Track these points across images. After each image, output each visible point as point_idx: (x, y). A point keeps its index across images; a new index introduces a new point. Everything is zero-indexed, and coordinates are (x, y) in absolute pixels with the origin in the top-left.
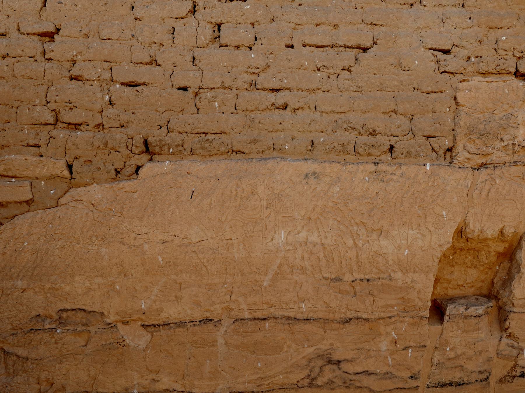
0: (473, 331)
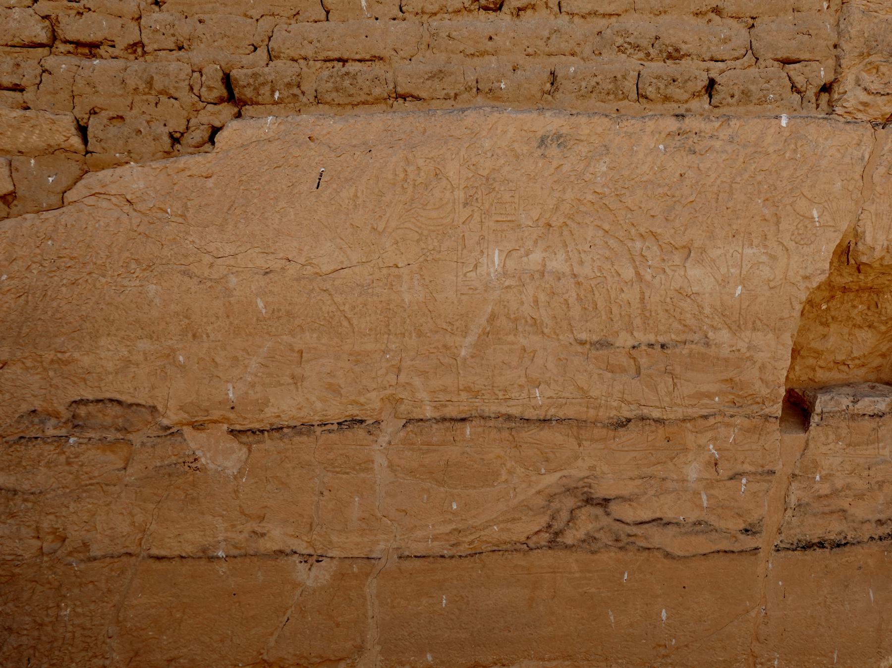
0: (867, 444)
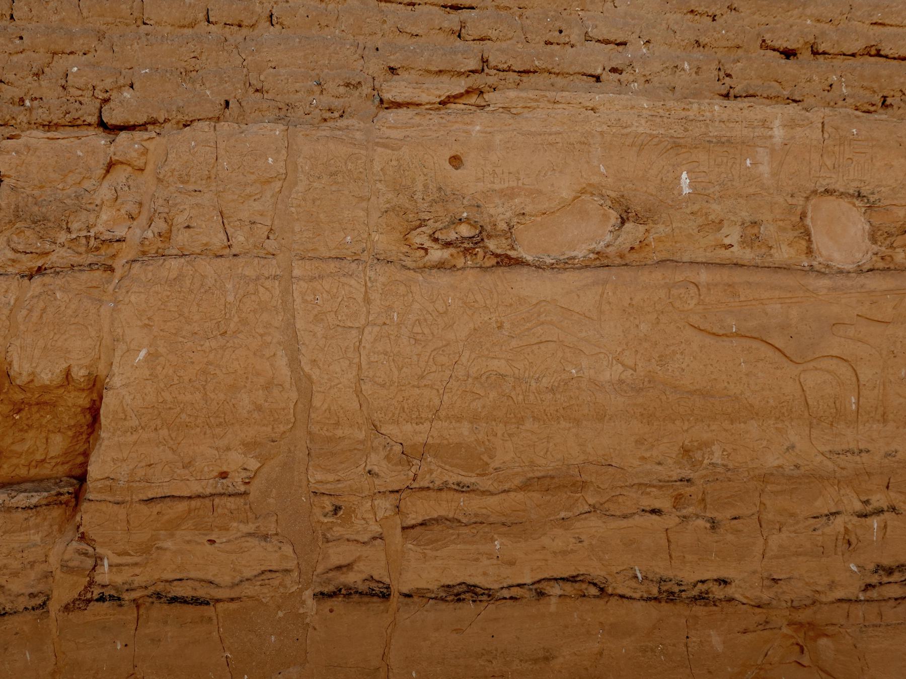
0: (21, 531)
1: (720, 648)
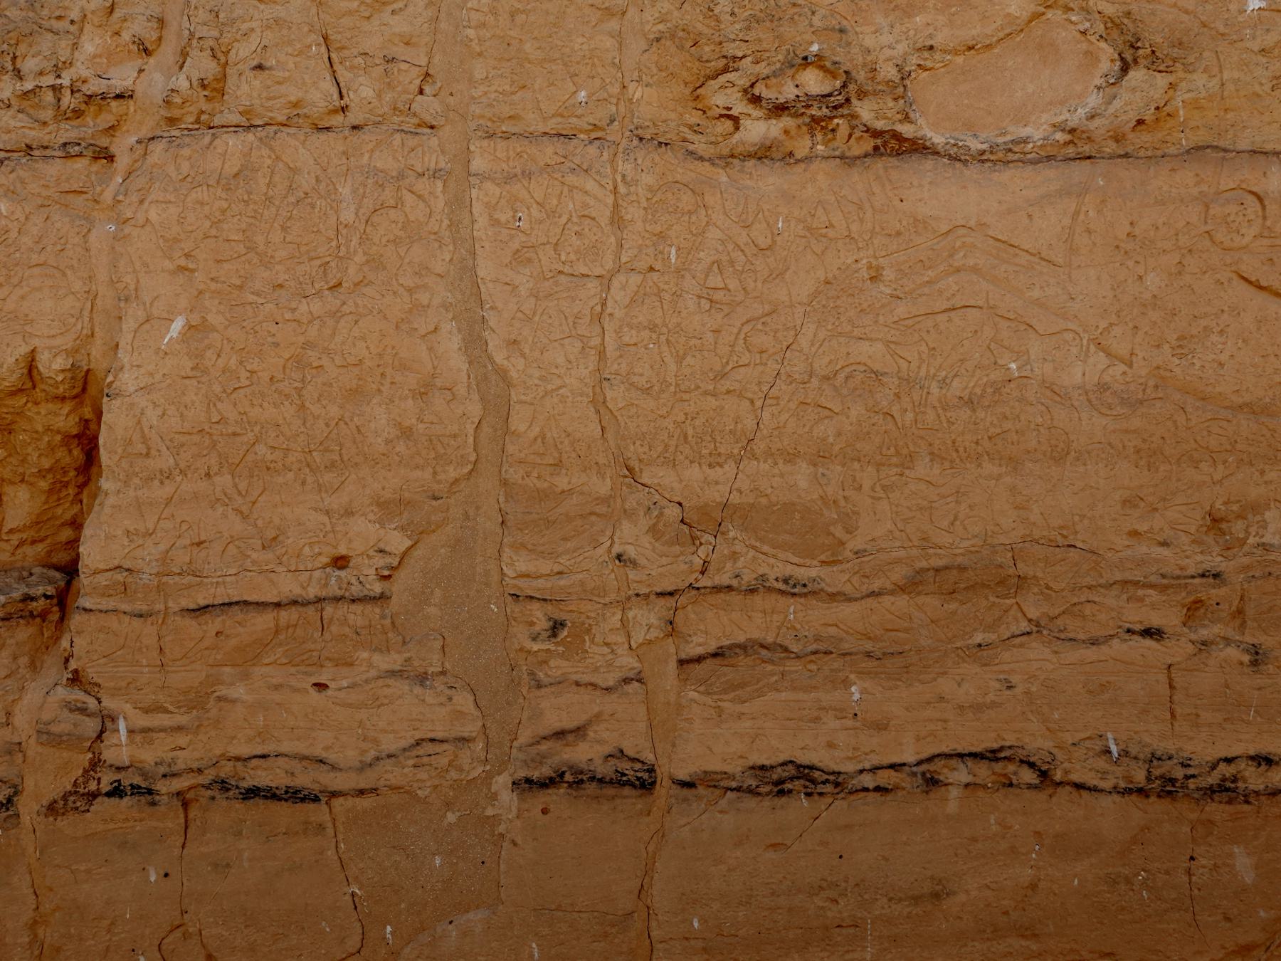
1: (1248, 880)
